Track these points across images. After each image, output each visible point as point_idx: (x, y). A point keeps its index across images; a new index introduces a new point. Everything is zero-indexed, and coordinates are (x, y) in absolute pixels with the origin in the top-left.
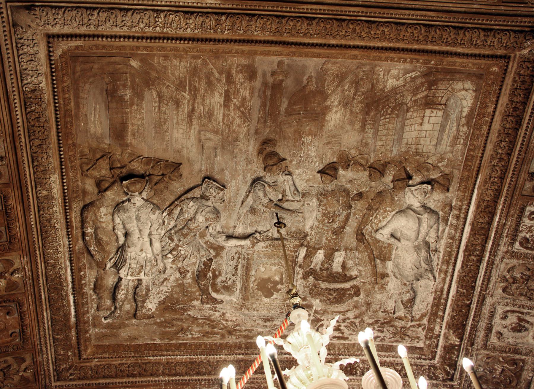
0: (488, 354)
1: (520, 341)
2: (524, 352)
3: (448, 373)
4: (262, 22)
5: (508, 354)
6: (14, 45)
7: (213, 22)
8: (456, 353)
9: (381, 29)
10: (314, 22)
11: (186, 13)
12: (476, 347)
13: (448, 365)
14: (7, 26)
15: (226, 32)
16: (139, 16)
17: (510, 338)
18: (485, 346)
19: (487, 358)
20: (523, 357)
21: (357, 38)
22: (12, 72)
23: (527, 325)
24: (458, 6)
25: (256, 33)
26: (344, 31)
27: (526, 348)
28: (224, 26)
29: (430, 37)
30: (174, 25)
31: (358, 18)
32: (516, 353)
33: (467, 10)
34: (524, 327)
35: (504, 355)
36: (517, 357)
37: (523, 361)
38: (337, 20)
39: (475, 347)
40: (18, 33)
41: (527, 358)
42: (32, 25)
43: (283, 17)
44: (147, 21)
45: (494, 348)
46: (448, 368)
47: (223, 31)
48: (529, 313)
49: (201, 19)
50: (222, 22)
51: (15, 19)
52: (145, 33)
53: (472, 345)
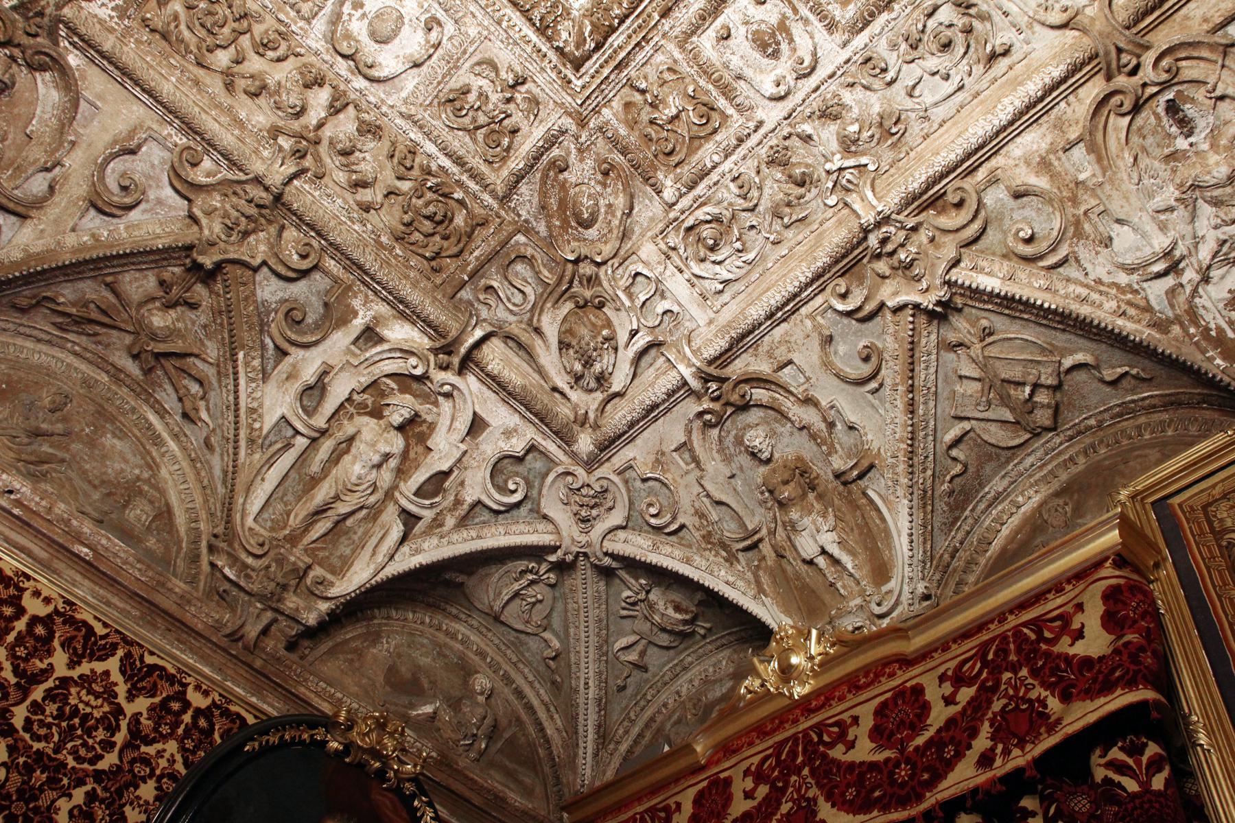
0: (675, 61)
1: (748, 73)
2: (738, 100)
3: (581, 42)
5: (710, 87)
8: (625, 5)
12: (666, 28)
13: (592, 24)
17: (741, 54)
18: (683, 40)
19: (669, 69)
20: (730, 111)
23: (784, 46)
27: (747, 97)
32: (724, 94)
34: (778, 43)
35: (702, 83)
36: (722, 103)
37: (725, 117)
39: (666, 24)
41: (736, 115)
45: (694, 56)
46: (589, 28)
48: (806, 22)
53: (665, 13)
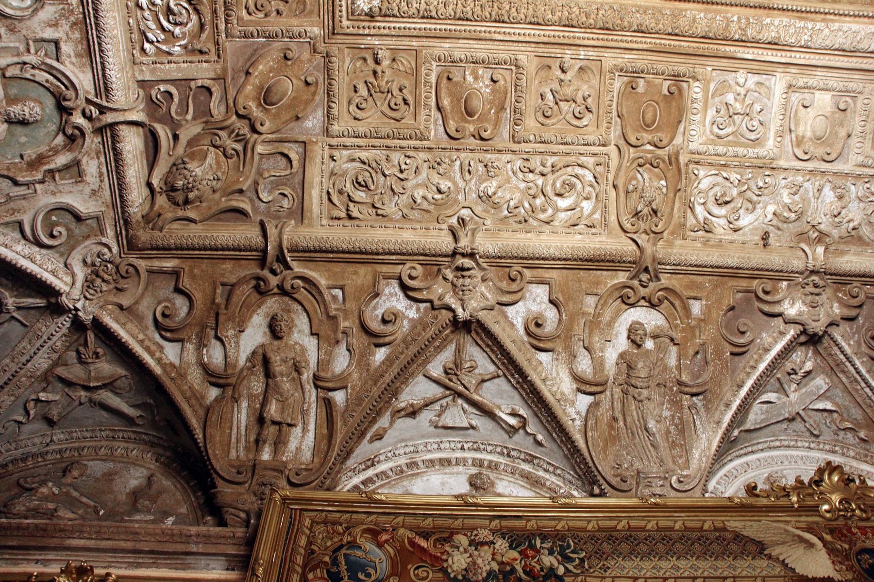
4: (694, 29)
7: (749, 32)
9: (556, 18)
10: (635, 27)
11: (776, 44)
15: (735, 18)
16: (827, 43)
21: (584, 6)
24: (467, 46)
25: (702, 15)
26: (600, 15)
28: (737, 27)
29: (495, 7)
30: (792, 31)
31: (583, 30)
33: (456, 41)
38: (608, 29)
43: (669, 34)
44: (820, 36)
47: (739, 19)
49: (760, 37)
50: (740, 32)
52: (823, 20)
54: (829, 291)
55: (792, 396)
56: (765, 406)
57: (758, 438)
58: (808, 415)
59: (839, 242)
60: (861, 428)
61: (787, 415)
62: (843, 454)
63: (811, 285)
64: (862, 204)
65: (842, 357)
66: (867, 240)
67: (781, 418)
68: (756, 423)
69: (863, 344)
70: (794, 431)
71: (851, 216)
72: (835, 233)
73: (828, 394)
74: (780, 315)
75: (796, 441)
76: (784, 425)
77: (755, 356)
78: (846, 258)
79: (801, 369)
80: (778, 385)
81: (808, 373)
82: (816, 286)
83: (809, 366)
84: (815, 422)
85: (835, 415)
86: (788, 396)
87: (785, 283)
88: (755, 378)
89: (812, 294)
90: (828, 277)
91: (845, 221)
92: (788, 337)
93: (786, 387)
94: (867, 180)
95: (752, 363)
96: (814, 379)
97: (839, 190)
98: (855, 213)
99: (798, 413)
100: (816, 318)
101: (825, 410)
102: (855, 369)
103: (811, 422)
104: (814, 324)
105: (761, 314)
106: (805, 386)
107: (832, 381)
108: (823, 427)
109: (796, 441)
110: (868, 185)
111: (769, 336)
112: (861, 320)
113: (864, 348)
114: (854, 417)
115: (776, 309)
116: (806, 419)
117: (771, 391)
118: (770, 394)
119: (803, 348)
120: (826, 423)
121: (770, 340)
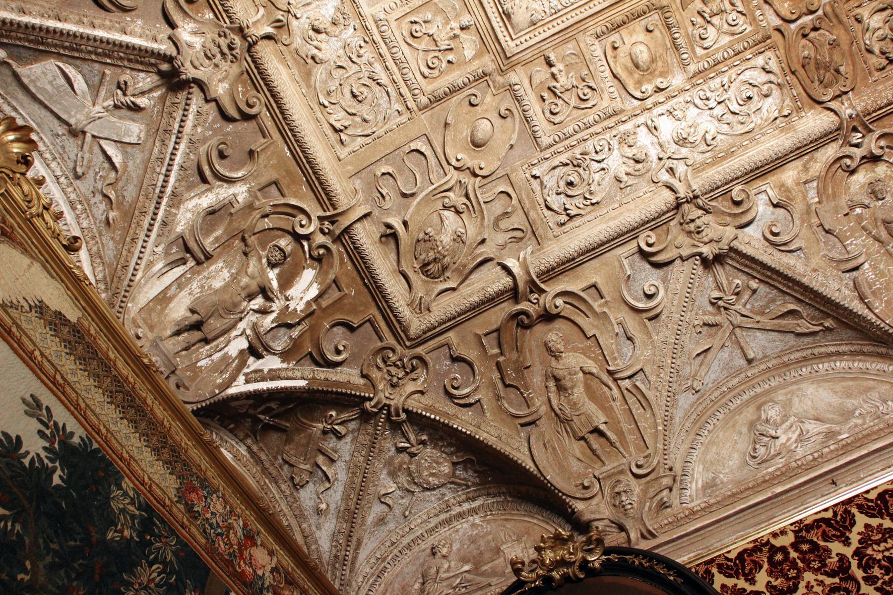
6: (555, 16)
14: (538, 30)
22: (587, 8)
40: (540, 17)
42: (524, 7)
51: (527, 26)
54: (235, 69)
55: (98, 108)
56: (62, 81)
57: (21, 105)
58: (91, 148)
59: (290, 52)
60: (118, 208)
61: (72, 121)
62: (78, 217)
63: (228, 41)
64: (341, 52)
65: (176, 126)
66: (312, 83)
67: (64, 117)
68: (33, 81)
69: (207, 146)
70: (63, 147)
71: (323, 46)
72: (298, 42)
73: (129, 149)
74: (172, 25)
75: (54, 159)
76: (61, 130)
77: (107, 23)
78: (281, 68)
79: (133, 95)
80: (97, 80)
81: (136, 108)
82: (231, 48)
83: (142, 101)
84: (90, 161)
85: (113, 175)
86: (94, 105)
87: (211, 15)
88: (81, 30)
89: (219, 47)
90: (249, 59)
91: (315, 43)
92: (155, 46)
93: (103, 93)
94: (367, 39)
95: (97, 22)
96: (134, 121)
97: (340, 16)
98: (329, 49)
99: (84, 133)
100: (197, 63)
101: (109, 159)
102: (175, 148)
103: (87, 156)
104: (188, 64)
105: (160, 7)
106: (120, 118)
107: (146, 141)
108: (90, 175)
109: (54, 159)
110: (363, 44)
111: (142, 28)
112: (230, 127)
113: (202, 150)
114: (125, 193)
115: (176, 17)
116: (86, 147)
117: (84, 76)
118: (80, 77)
119: (156, 78)
120: (97, 173)
121: (138, 30)
